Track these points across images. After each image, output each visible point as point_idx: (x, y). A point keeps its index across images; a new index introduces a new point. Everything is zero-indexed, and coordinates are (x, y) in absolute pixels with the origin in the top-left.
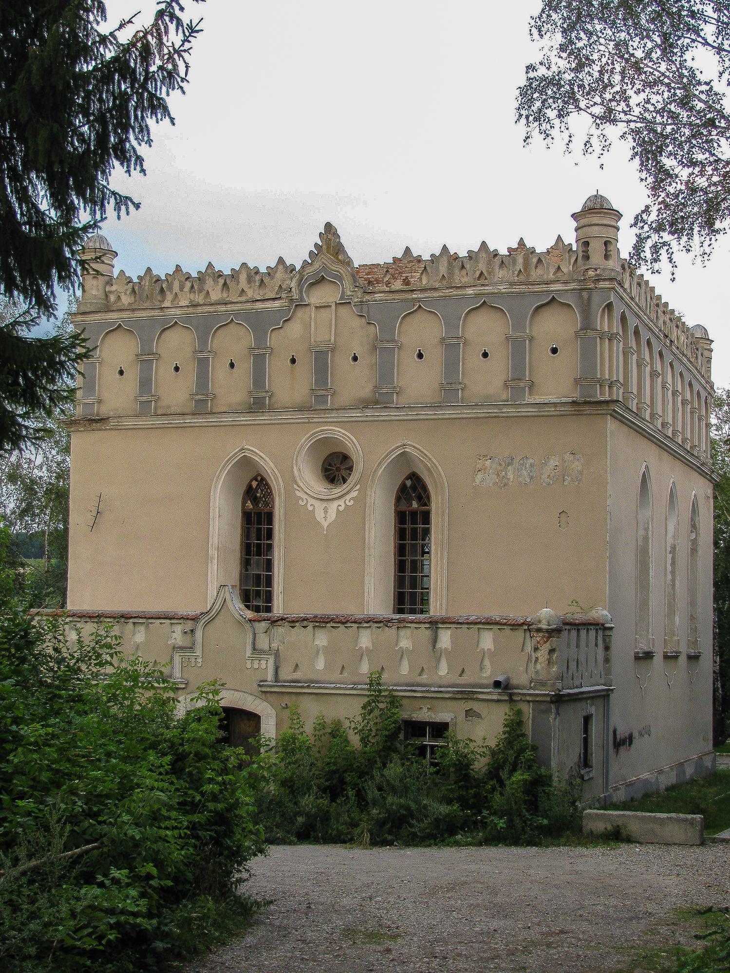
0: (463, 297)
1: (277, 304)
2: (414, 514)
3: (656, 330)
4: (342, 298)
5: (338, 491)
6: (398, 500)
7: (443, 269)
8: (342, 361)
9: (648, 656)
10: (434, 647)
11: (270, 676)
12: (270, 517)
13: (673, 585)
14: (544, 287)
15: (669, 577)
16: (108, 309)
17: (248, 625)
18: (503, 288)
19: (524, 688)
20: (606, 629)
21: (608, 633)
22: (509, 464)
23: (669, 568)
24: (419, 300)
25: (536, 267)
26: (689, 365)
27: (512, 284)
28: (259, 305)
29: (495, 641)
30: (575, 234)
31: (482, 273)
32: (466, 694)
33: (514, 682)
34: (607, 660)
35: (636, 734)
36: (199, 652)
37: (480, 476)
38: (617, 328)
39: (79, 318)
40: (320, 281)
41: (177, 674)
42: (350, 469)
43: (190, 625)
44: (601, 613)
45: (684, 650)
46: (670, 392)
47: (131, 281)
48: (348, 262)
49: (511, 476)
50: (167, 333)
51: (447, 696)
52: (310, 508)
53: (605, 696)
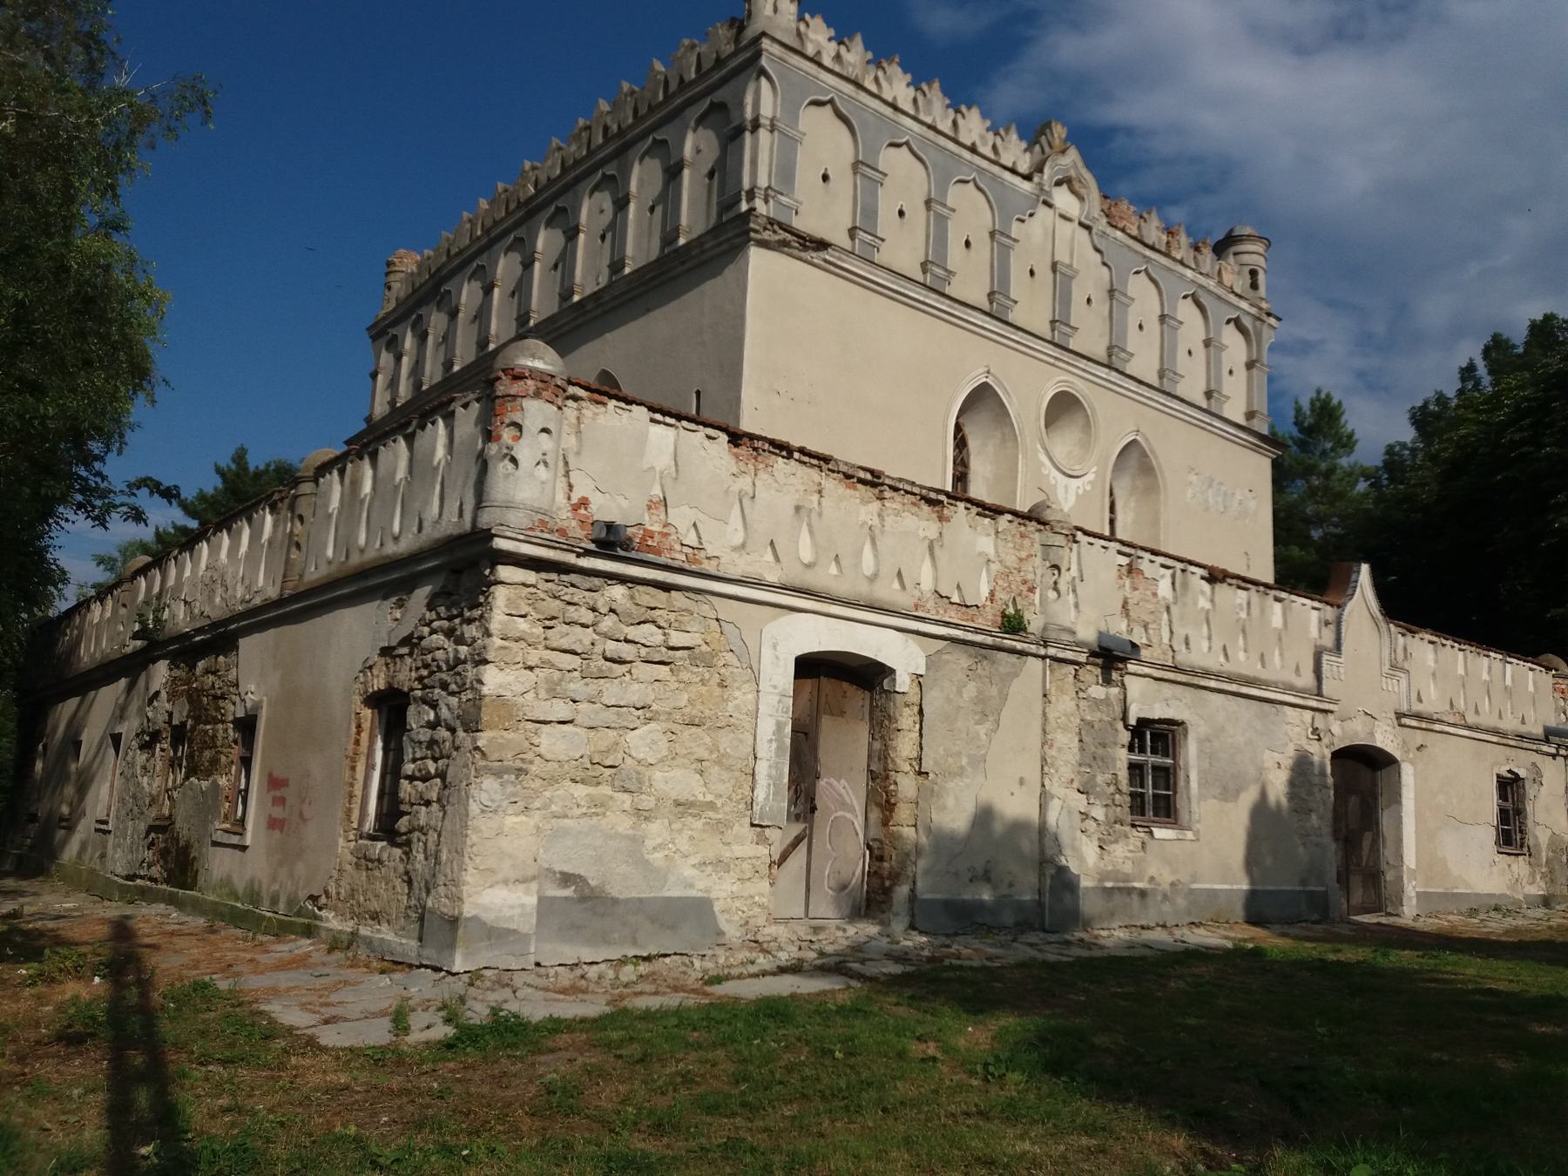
0: (1182, 276)
4: (1086, 218)
8: (1078, 299)
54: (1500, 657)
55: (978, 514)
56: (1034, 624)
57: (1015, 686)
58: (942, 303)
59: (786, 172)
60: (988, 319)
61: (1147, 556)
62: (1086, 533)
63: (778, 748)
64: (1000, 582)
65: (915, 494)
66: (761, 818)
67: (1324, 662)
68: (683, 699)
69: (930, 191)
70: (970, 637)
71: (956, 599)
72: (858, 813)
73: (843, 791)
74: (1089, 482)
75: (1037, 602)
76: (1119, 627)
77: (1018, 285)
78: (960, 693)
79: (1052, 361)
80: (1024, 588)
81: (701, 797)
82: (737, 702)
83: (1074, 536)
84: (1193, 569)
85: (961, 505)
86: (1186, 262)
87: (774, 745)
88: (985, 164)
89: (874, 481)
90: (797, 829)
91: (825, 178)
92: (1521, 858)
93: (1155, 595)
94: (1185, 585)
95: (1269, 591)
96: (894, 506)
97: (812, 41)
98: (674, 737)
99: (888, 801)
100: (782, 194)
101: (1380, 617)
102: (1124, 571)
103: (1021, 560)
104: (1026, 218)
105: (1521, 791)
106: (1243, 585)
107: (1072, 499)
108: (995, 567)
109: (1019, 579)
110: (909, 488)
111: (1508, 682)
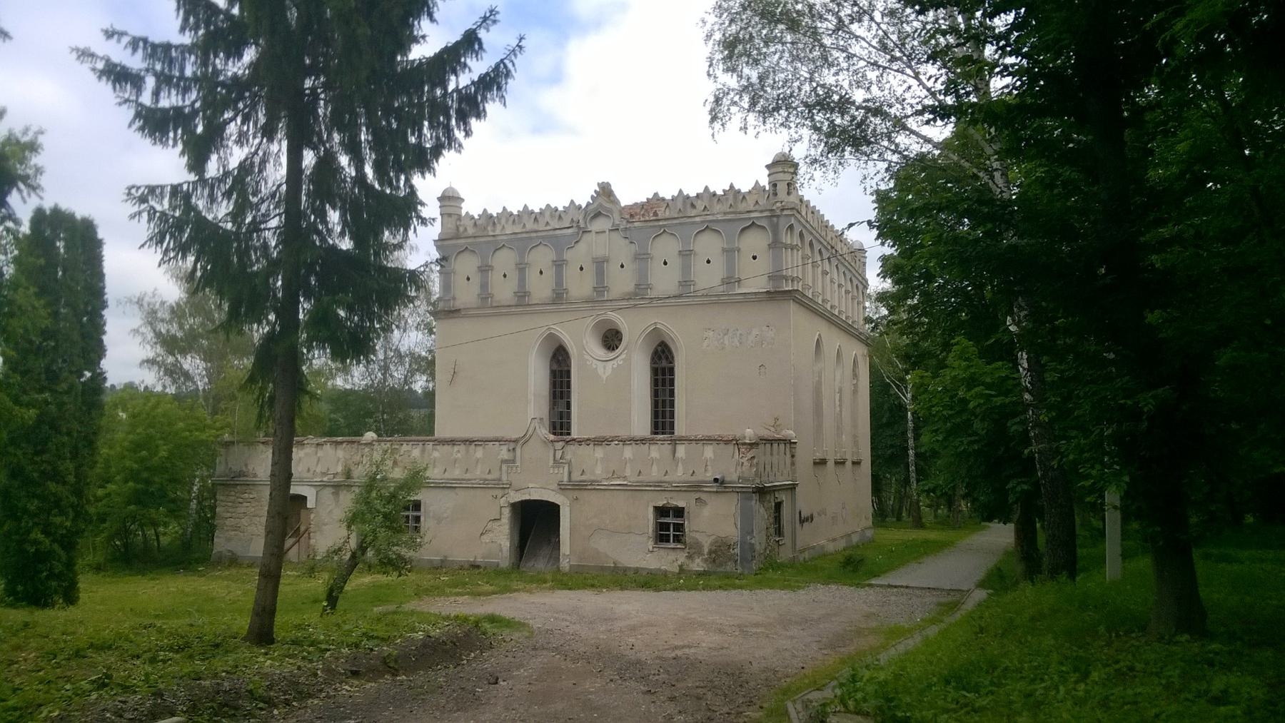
0: (693, 223)
1: (570, 231)
2: (663, 369)
3: (825, 244)
4: (613, 226)
5: (612, 355)
6: (653, 359)
7: (680, 205)
9: (821, 463)
10: (674, 456)
11: (566, 479)
12: (569, 372)
13: (841, 415)
14: (746, 216)
15: (838, 409)
16: (457, 237)
17: (550, 445)
18: (720, 217)
19: (735, 483)
20: (791, 443)
21: (793, 446)
22: (725, 334)
23: (837, 403)
24: (664, 226)
25: (742, 202)
26: (849, 267)
27: (725, 213)
28: (558, 232)
29: (714, 452)
30: (767, 179)
31: (705, 207)
32: (696, 487)
33: (727, 479)
34: (793, 464)
35: (815, 515)
36: (518, 464)
37: (706, 342)
38: (796, 241)
39: (439, 243)
40: (598, 215)
41: (504, 478)
42: (621, 340)
43: (512, 446)
44: (790, 433)
45: (850, 458)
46: (836, 285)
47: (472, 218)
48: (616, 202)
49: (726, 342)
50: (498, 252)
51: (684, 489)
52: (595, 367)
53: (792, 488)
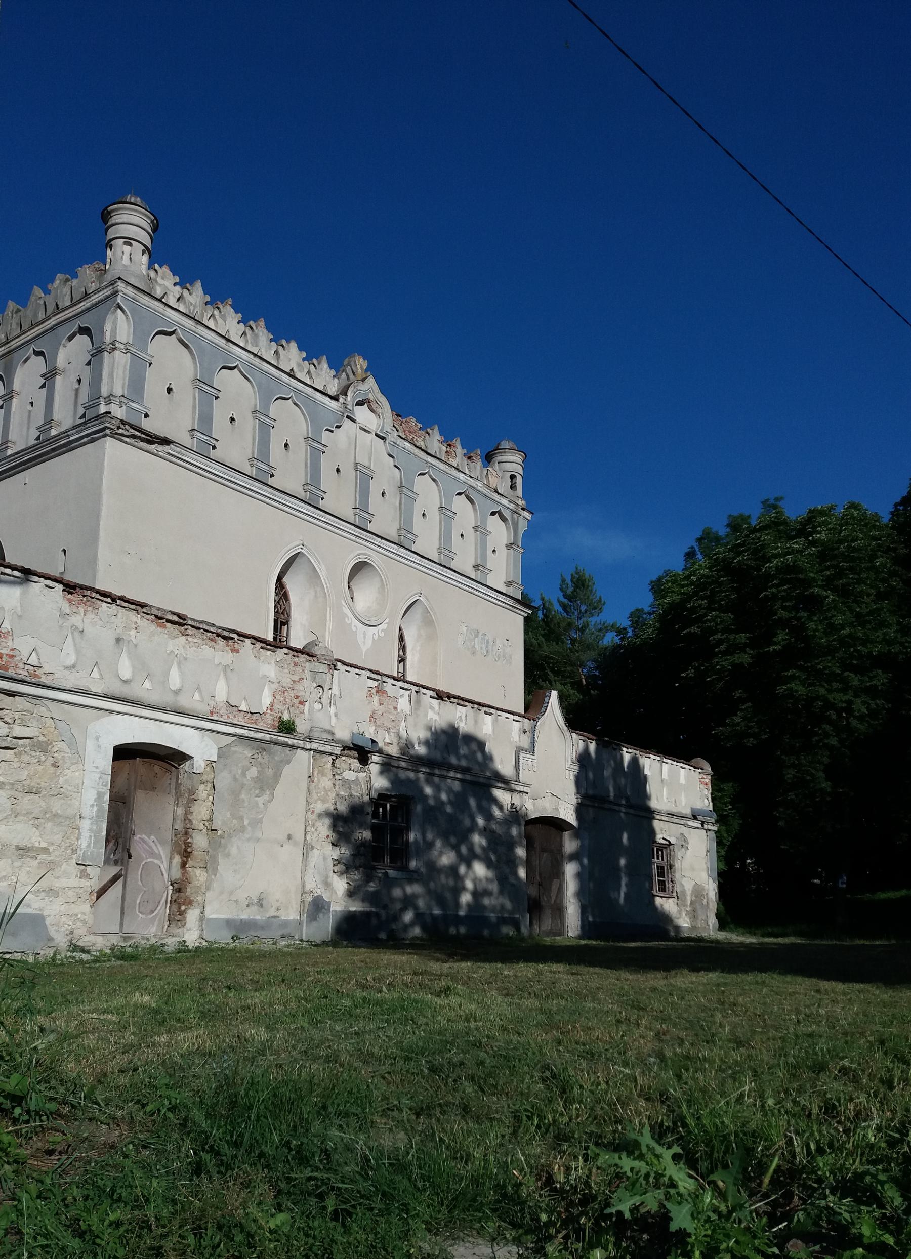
0: (456, 479)
1: (333, 404)
4: (381, 431)
8: (375, 489)
54: (659, 758)
55: (261, 648)
56: (302, 727)
57: (287, 770)
58: (266, 491)
59: (137, 385)
60: (302, 504)
61: (391, 681)
62: (344, 664)
63: (98, 811)
64: (278, 697)
65: (212, 633)
66: (83, 860)
67: (521, 758)
68: (24, 774)
69: (256, 405)
70: (252, 734)
71: (243, 707)
72: (164, 859)
73: (152, 844)
74: (382, 630)
75: (306, 711)
76: (370, 732)
77: (327, 480)
78: (244, 774)
79: (353, 538)
80: (296, 701)
81: (37, 844)
82: (66, 778)
83: (335, 666)
84: (424, 691)
85: (248, 641)
86: (459, 467)
87: (95, 808)
88: (300, 386)
89: (180, 621)
90: (114, 871)
91: (169, 390)
92: (671, 900)
93: (395, 708)
94: (418, 702)
95: (481, 708)
96: (195, 640)
97: (160, 285)
98: (16, 801)
99: (185, 850)
100: (133, 401)
101: (566, 728)
102: (374, 691)
103: (294, 681)
104: (334, 429)
105: (672, 853)
106: (462, 703)
107: (369, 642)
108: (275, 686)
109: (293, 695)
110: (207, 628)
111: (665, 775)
